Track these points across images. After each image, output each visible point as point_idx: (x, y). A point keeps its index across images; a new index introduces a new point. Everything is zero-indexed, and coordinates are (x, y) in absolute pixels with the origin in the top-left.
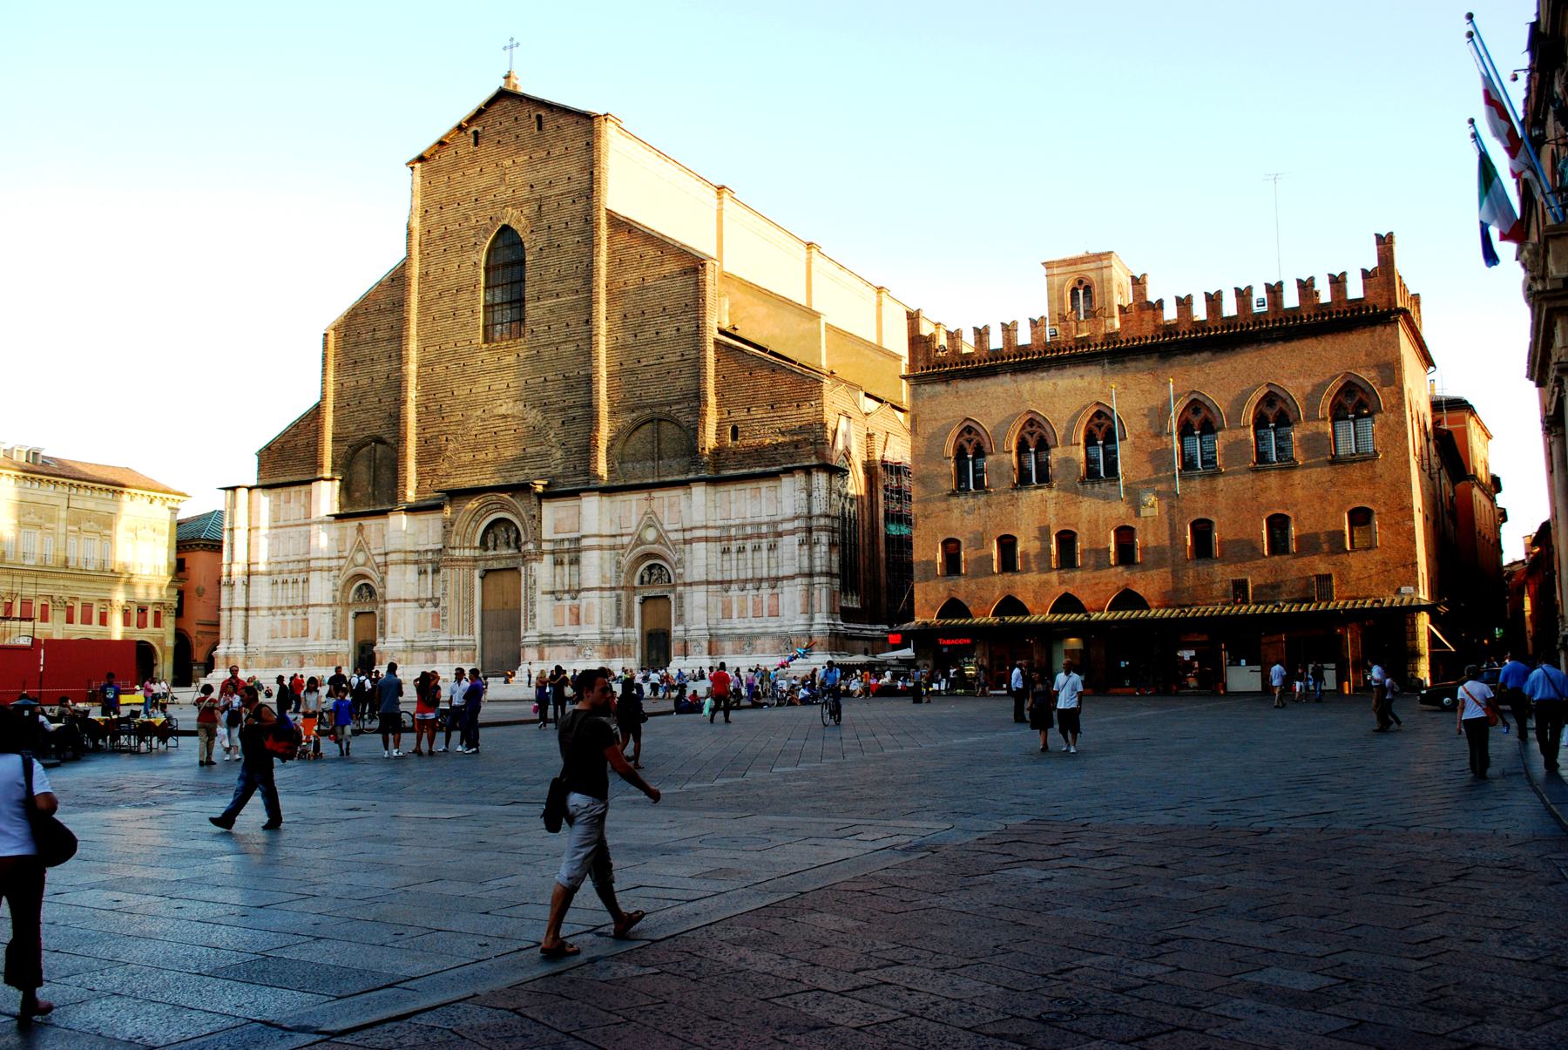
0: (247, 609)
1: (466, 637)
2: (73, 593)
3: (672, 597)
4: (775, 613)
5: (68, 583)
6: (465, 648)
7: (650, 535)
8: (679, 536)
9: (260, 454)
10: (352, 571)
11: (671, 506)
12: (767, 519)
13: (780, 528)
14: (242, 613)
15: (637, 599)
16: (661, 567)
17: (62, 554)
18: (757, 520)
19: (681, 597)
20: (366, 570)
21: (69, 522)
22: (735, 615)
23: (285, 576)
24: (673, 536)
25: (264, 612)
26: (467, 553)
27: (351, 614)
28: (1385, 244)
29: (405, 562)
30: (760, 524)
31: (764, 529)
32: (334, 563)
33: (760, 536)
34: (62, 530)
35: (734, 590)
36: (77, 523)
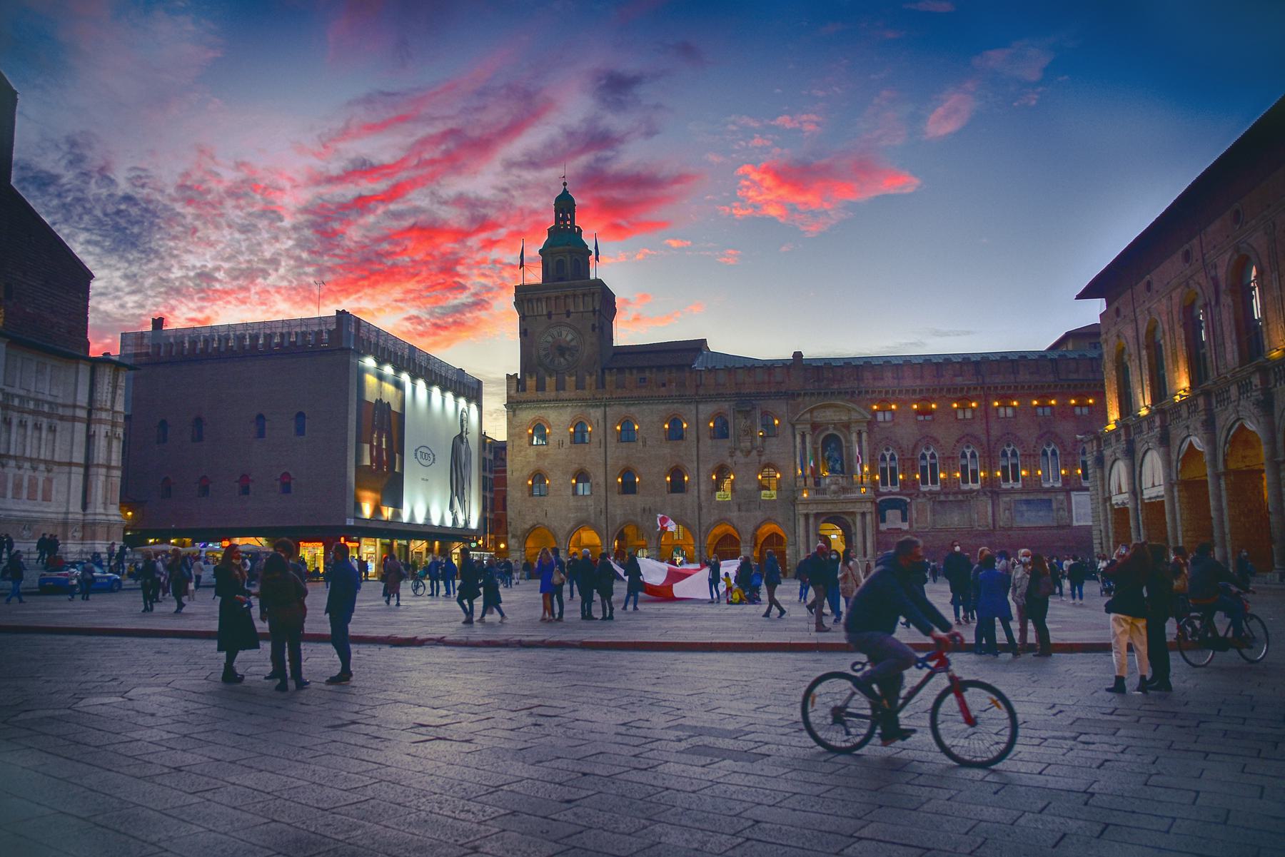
4: (47, 498)
12: (49, 399)
13: (60, 411)
22: (9, 494)
31: (46, 408)
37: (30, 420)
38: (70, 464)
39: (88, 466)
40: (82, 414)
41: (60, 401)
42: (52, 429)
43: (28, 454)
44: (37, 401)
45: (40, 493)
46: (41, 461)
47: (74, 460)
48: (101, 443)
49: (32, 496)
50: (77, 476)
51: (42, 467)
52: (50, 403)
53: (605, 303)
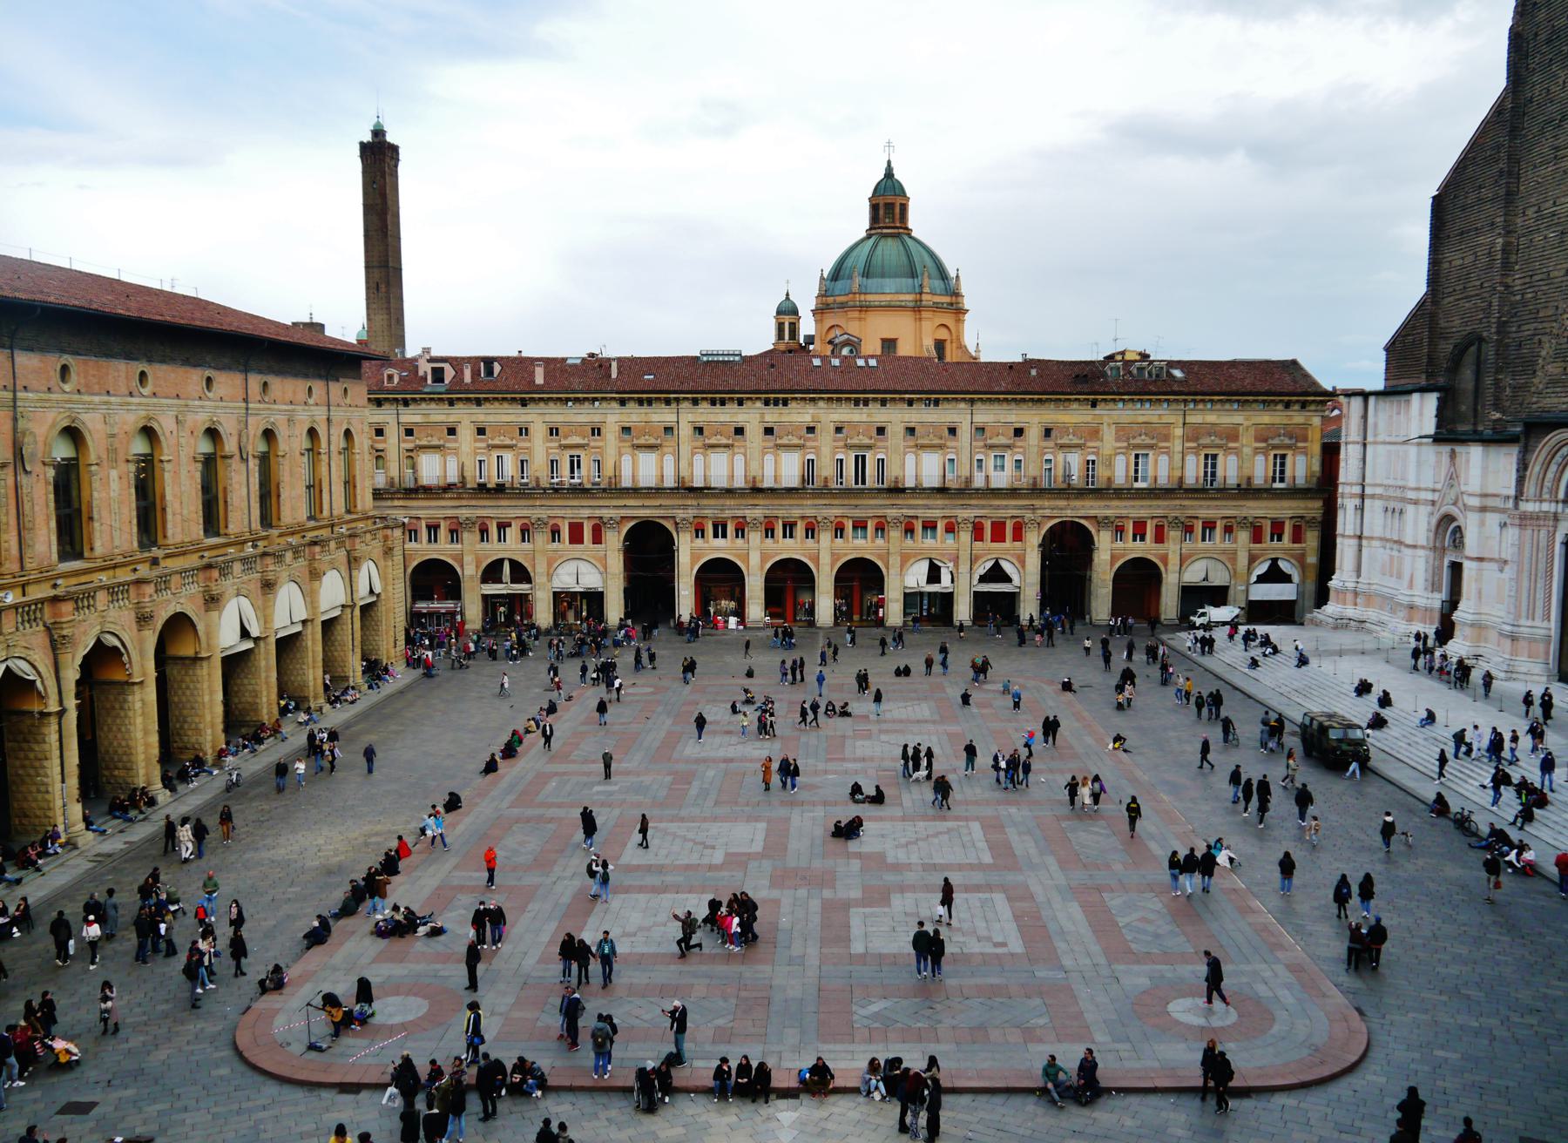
0: (1360, 537)
1: (1538, 623)
2: (1191, 512)
5: (1186, 503)
6: (1532, 640)
9: (1388, 349)
10: (1443, 510)
14: (1354, 542)
17: (1178, 473)
20: (1454, 511)
21: (1185, 438)
23: (1391, 505)
25: (1376, 543)
26: (1545, 507)
27: (1446, 563)
29: (1483, 509)
32: (1430, 496)
34: (1178, 448)
36: (1196, 439)
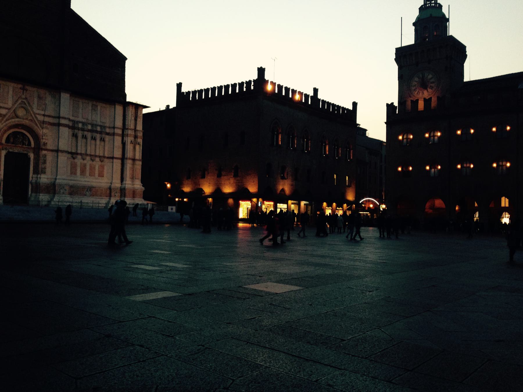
3: (32, 156)
4: (101, 175)
7: (21, 113)
8: (47, 119)
11: (40, 98)
12: (100, 124)
13: (108, 130)
15: (4, 153)
16: (23, 134)
18: (95, 123)
19: (45, 156)
24: (41, 118)
28: (355, 104)
30: (97, 125)
31: (99, 129)
33: (97, 132)
35: (79, 161)
37: (89, 135)
38: (113, 158)
39: (123, 159)
40: (119, 132)
41: (108, 125)
42: (102, 140)
43: (97, 154)
44: (92, 125)
45: (97, 172)
46: (96, 156)
47: (115, 156)
48: (129, 147)
49: (92, 174)
50: (117, 164)
51: (98, 159)
52: (101, 126)
53: (458, 52)
